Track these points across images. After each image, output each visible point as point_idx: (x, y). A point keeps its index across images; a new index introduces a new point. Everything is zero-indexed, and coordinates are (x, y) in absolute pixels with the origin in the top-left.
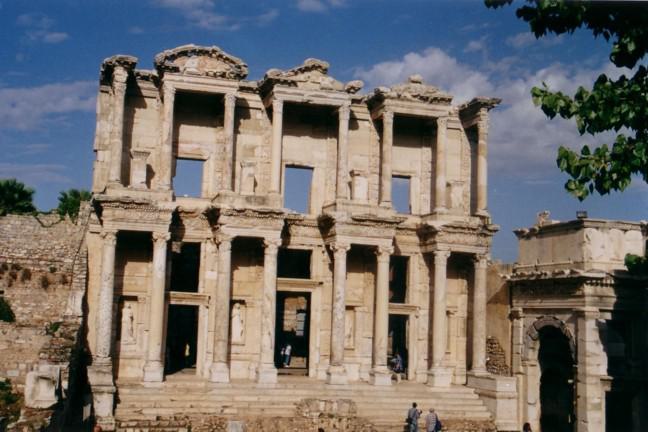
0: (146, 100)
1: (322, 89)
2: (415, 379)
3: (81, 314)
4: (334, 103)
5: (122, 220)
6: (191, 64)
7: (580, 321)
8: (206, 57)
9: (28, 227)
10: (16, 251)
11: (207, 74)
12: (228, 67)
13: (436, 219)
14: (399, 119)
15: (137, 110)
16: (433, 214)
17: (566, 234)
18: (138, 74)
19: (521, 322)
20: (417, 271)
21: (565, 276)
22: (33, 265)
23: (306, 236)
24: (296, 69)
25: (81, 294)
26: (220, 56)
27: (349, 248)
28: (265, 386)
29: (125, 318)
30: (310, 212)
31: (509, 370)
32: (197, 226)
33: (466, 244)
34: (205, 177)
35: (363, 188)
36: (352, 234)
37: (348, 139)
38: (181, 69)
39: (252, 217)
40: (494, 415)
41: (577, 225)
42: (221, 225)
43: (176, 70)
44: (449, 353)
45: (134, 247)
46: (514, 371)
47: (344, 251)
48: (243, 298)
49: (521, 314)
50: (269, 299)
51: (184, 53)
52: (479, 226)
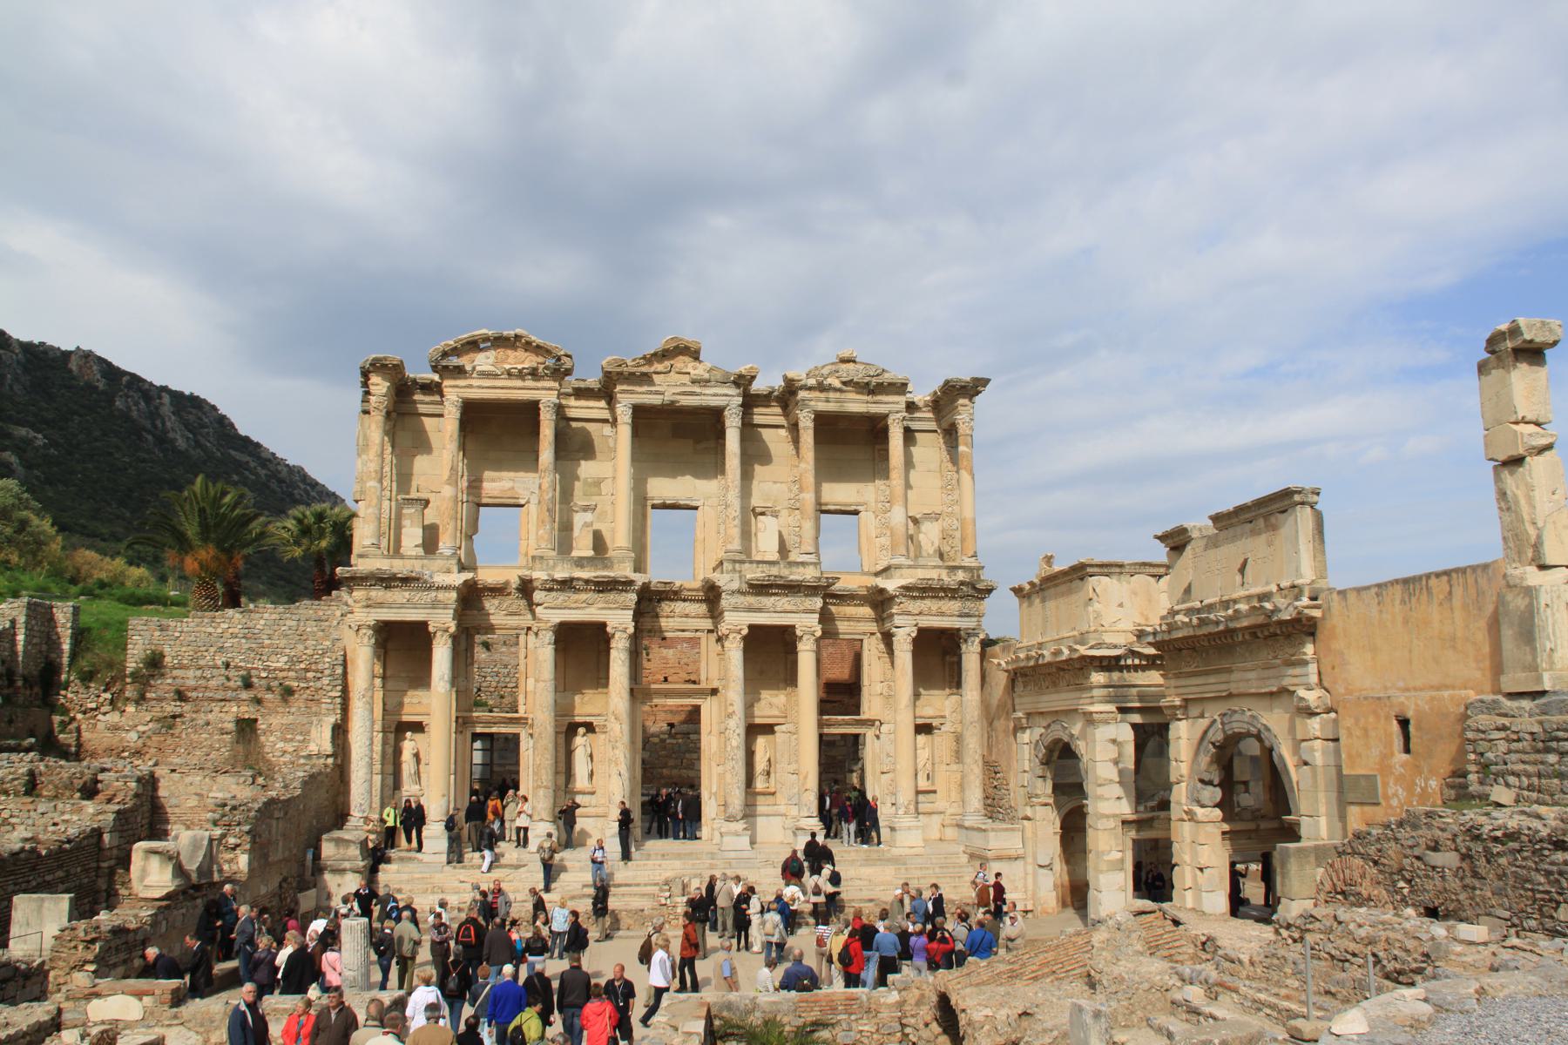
5: (381, 605)
6: (484, 361)
7: (1089, 730)
8: (506, 347)
9: (289, 623)
10: (273, 658)
11: (509, 374)
12: (541, 359)
16: (885, 571)
18: (414, 381)
19: (1025, 737)
20: (875, 661)
22: (297, 679)
23: (687, 616)
25: (332, 720)
26: (529, 343)
27: (745, 632)
29: (407, 756)
32: (514, 608)
33: (942, 614)
36: (750, 609)
38: (468, 368)
44: (934, 792)
48: (588, 719)
51: (473, 345)
52: (962, 583)
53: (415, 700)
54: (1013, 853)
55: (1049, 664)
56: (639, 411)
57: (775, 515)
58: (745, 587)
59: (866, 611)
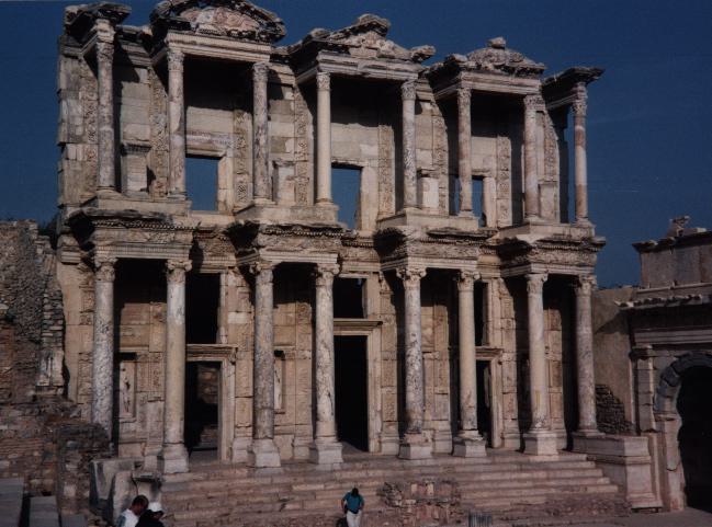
0: (137, 70)
1: (382, 56)
2: (503, 445)
3: (61, 383)
6: (205, 18)
11: (229, 34)
12: (255, 24)
14: (477, 96)
15: (124, 83)
20: (497, 300)
23: (358, 260)
24: (348, 29)
26: (247, 8)
27: (424, 274)
28: (328, 468)
30: (360, 228)
31: (632, 428)
33: (566, 264)
34: (221, 182)
35: (434, 193)
36: (428, 255)
37: (414, 124)
38: (193, 26)
40: (623, 488)
42: (259, 247)
43: (184, 26)
45: (139, 282)
46: (643, 427)
47: (419, 278)
49: (650, 353)
50: (326, 347)
52: (583, 239)
53: (128, 333)
54: (642, 459)
55: (703, 305)
56: (337, 81)
57: (436, 176)
58: (425, 237)
59: (493, 259)
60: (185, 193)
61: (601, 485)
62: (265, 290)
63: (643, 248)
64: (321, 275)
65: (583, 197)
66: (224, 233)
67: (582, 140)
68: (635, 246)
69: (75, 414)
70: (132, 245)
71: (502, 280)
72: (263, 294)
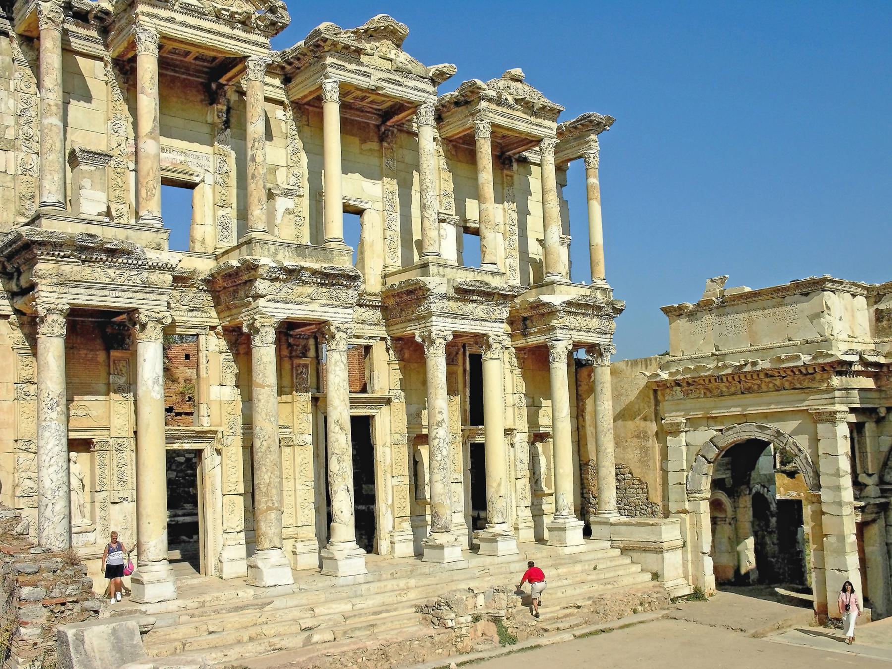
4: (414, 96)
13: (552, 292)
17: (780, 305)
19: (683, 438)
21: (800, 363)
23: (363, 322)
27: (451, 338)
33: (589, 330)
34: (198, 217)
36: (453, 315)
39: (309, 284)
41: (810, 288)
42: (257, 297)
46: (673, 507)
47: (444, 342)
53: (81, 412)
55: (762, 370)
60: (161, 219)
61: (633, 576)
62: (265, 353)
63: (674, 312)
64: (333, 337)
65: (600, 256)
66: (205, 281)
67: (596, 194)
68: (662, 309)
69: (19, 529)
70: (90, 285)
71: (514, 350)
72: (264, 359)
